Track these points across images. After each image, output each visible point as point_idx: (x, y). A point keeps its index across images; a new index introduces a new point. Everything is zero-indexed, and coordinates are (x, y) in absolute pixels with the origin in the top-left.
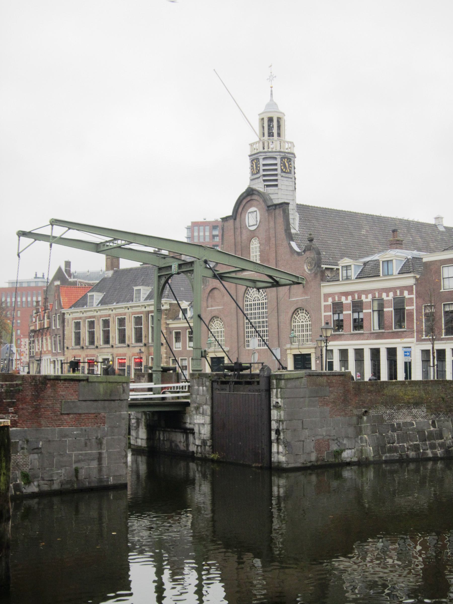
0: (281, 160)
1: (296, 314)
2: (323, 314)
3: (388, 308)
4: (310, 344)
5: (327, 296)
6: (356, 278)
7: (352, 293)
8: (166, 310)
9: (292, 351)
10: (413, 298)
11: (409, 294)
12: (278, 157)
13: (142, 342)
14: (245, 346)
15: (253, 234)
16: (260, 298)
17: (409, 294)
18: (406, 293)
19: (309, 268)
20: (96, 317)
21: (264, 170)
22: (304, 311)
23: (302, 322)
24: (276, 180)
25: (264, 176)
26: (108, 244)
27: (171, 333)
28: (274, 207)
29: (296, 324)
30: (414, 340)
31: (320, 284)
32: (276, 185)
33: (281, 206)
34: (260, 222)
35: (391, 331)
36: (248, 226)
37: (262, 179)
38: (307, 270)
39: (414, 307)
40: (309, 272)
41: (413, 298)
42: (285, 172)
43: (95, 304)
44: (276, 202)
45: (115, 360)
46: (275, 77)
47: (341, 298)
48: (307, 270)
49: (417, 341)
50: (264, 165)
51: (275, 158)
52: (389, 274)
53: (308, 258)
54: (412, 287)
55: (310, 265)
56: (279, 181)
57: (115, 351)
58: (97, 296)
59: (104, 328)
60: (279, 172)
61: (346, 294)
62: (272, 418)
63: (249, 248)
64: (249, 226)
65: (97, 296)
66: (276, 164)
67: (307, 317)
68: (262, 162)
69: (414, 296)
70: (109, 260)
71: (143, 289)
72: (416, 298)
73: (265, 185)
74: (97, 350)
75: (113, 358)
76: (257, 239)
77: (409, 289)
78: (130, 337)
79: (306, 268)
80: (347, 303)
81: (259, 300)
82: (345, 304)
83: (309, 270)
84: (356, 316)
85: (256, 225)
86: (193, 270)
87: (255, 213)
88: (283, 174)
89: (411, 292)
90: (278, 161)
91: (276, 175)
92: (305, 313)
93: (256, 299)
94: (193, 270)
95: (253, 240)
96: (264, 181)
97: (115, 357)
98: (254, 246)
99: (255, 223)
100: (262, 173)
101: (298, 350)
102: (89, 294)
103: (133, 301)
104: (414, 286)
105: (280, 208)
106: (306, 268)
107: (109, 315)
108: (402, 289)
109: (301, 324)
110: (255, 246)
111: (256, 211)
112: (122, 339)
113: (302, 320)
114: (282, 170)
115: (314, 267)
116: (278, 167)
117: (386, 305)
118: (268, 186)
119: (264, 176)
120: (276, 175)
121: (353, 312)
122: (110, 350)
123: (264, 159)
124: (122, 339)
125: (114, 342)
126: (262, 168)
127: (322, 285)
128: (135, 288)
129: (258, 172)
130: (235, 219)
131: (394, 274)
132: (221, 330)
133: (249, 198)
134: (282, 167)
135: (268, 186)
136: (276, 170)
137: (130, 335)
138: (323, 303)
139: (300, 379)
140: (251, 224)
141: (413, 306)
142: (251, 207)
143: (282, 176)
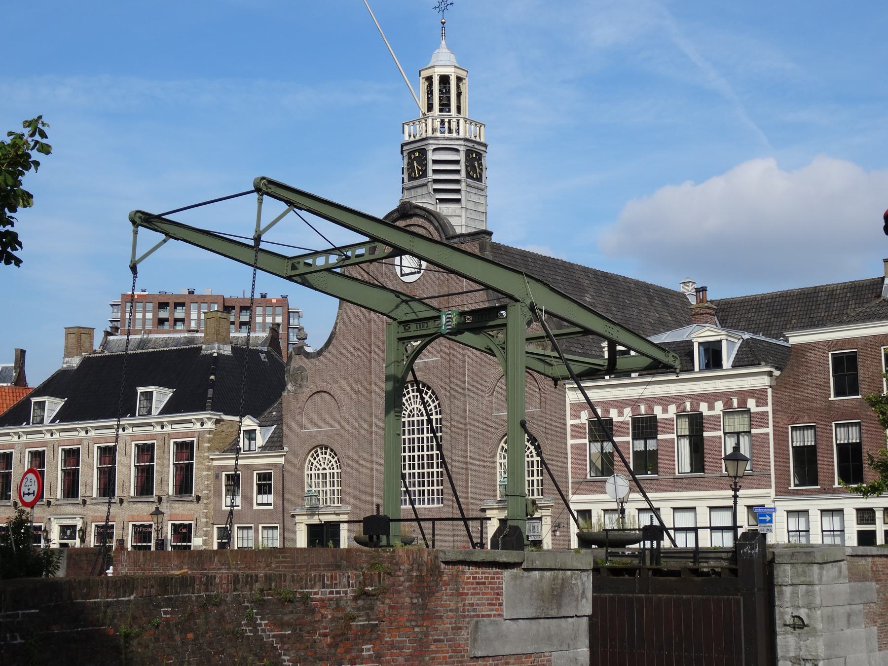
2: (570, 442)
3: (711, 430)
7: (634, 403)
8: (210, 432)
10: (767, 412)
11: (757, 406)
12: (462, 148)
13: (152, 494)
17: (757, 406)
18: (751, 404)
20: (50, 445)
22: (328, 451)
23: (324, 469)
24: (458, 191)
25: (436, 181)
26: (310, 261)
27: (217, 476)
29: (313, 472)
30: (772, 492)
32: (458, 201)
33: (475, 237)
35: (719, 475)
36: (399, 275)
39: (770, 430)
41: (767, 412)
42: (472, 178)
43: (156, 410)
44: (458, 231)
45: (88, 529)
46: (452, 4)
47: (608, 411)
50: (435, 162)
51: (457, 150)
54: (764, 391)
56: (463, 193)
57: (89, 510)
58: (53, 405)
59: (65, 466)
60: (462, 176)
62: (780, 652)
64: (402, 275)
65: (53, 405)
66: (457, 162)
67: (333, 461)
68: (431, 156)
69: (769, 409)
70: (73, 336)
71: (158, 392)
72: (773, 411)
74: (51, 509)
75: (85, 524)
77: (759, 395)
78: (126, 485)
82: (618, 422)
84: (640, 445)
85: (419, 272)
86: (505, 325)
89: (761, 402)
90: (462, 157)
91: (458, 182)
93: (415, 412)
94: (505, 325)
96: (436, 191)
97: (89, 523)
100: (431, 176)
102: (34, 400)
103: (133, 415)
104: (770, 391)
105: (473, 240)
107: (80, 442)
108: (743, 395)
109: (321, 472)
112: (107, 487)
116: (462, 167)
117: (706, 426)
118: (442, 201)
119: (436, 181)
120: (458, 182)
121: (633, 439)
122: (80, 509)
124: (107, 487)
125: (88, 494)
126: (431, 167)
128: (140, 390)
129: (424, 174)
132: (332, 471)
135: (442, 201)
136: (457, 172)
137: (126, 480)
138: (570, 422)
139: (838, 564)
140: (406, 270)
143: (468, 185)
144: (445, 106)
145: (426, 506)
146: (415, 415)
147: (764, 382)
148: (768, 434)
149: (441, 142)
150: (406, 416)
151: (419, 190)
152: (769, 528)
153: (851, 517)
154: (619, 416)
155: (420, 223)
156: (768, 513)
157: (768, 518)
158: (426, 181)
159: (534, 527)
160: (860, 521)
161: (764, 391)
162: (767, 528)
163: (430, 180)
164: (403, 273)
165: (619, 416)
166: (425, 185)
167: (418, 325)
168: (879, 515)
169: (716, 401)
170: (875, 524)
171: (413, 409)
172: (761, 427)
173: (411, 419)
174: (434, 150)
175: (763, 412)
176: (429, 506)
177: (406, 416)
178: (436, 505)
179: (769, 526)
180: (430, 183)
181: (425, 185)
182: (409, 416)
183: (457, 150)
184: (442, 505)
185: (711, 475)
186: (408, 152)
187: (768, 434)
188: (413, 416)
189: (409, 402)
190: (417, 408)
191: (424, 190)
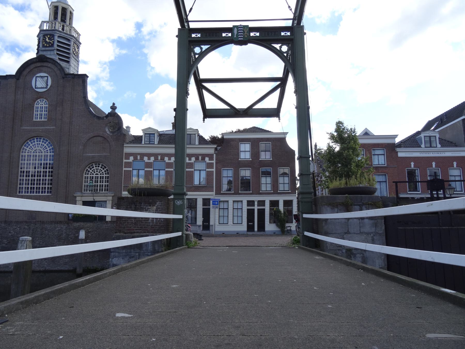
0: (73, 44)
1: (90, 167)
4: (107, 193)
5: (128, 155)
6: (158, 144)
9: (82, 198)
10: (213, 163)
14: (17, 192)
15: (40, 96)
16: (43, 151)
18: (207, 159)
19: (110, 130)
21: (58, 46)
24: (68, 58)
25: (58, 50)
28: (73, 76)
30: (214, 193)
31: (124, 144)
34: (51, 86)
35: (192, 186)
37: (55, 52)
38: (108, 132)
39: (214, 170)
40: (111, 134)
41: (213, 163)
42: (75, 54)
48: (108, 132)
49: (216, 194)
50: (58, 42)
51: (69, 40)
52: (192, 143)
53: (110, 122)
54: (213, 155)
55: (112, 128)
61: (149, 155)
63: (33, 107)
66: (69, 45)
68: (56, 38)
69: (214, 162)
72: (216, 163)
73: (58, 58)
76: (45, 100)
79: (107, 130)
80: (149, 162)
81: (42, 152)
83: (111, 132)
85: (46, 88)
87: (46, 78)
88: (74, 56)
91: (69, 54)
92: (101, 167)
95: (39, 100)
98: (39, 106)
99: (45, 86)
101: (92, 198)
104: (215, 155)
106: (107, 130)
110: (42, 106)
111: (47, 77)
113: (96, 173)
114: (73, 52)
115: (117, 131)
118: (60, 59)
119: (58, 50)
123: (59, 37)
126: (56, 43)
127: (124, 145)
130: (18, 79)
131: (196, 144)
133: (39, 64)
134: (74, 50)
135: (60, 59)
141: (213, 169)
142: (40, 72)
143: (73, 57)
144: (63, 20)
145: (40, 194)
146: (38, 152)
147: (212, 151)
148: (213, 171)
149: (62, 34)
150: (32, 153)
151: (49, 53)
152: (217, 207)
153: (245, 203)
154: (148, 160)
155: (49, 66)
156: (216, 201)
157: (217, 203)
158: (53, 49)
159: (102, 205)
160: (248, 205)
161: (213, 155)
162: (216, 207)
163: (56, 49)
164: (37, 87)
165: (148, 160)
166: (53, 50)
167: (208, 34)
168: (256, 203)
169: (192, 157)
170: (254, 206)
171: (37, 149)
172: (211, 168)
173: (35, 154)
174: (59, 37)
175: (211, 163)
176: (42, 194)
177: (32, 153)
178: (46, 194)
179: (217, 206)
180: (55, 50)
181: (53, 50)
182: (34, 152)
183: (69, 40)
184: (51, 194)
185: (188, 186)
186: (44, 34)
187: (213, 171)
188: (36, 153)
189: (34, 146)
190: (39, 149)
191: (52, 53)
